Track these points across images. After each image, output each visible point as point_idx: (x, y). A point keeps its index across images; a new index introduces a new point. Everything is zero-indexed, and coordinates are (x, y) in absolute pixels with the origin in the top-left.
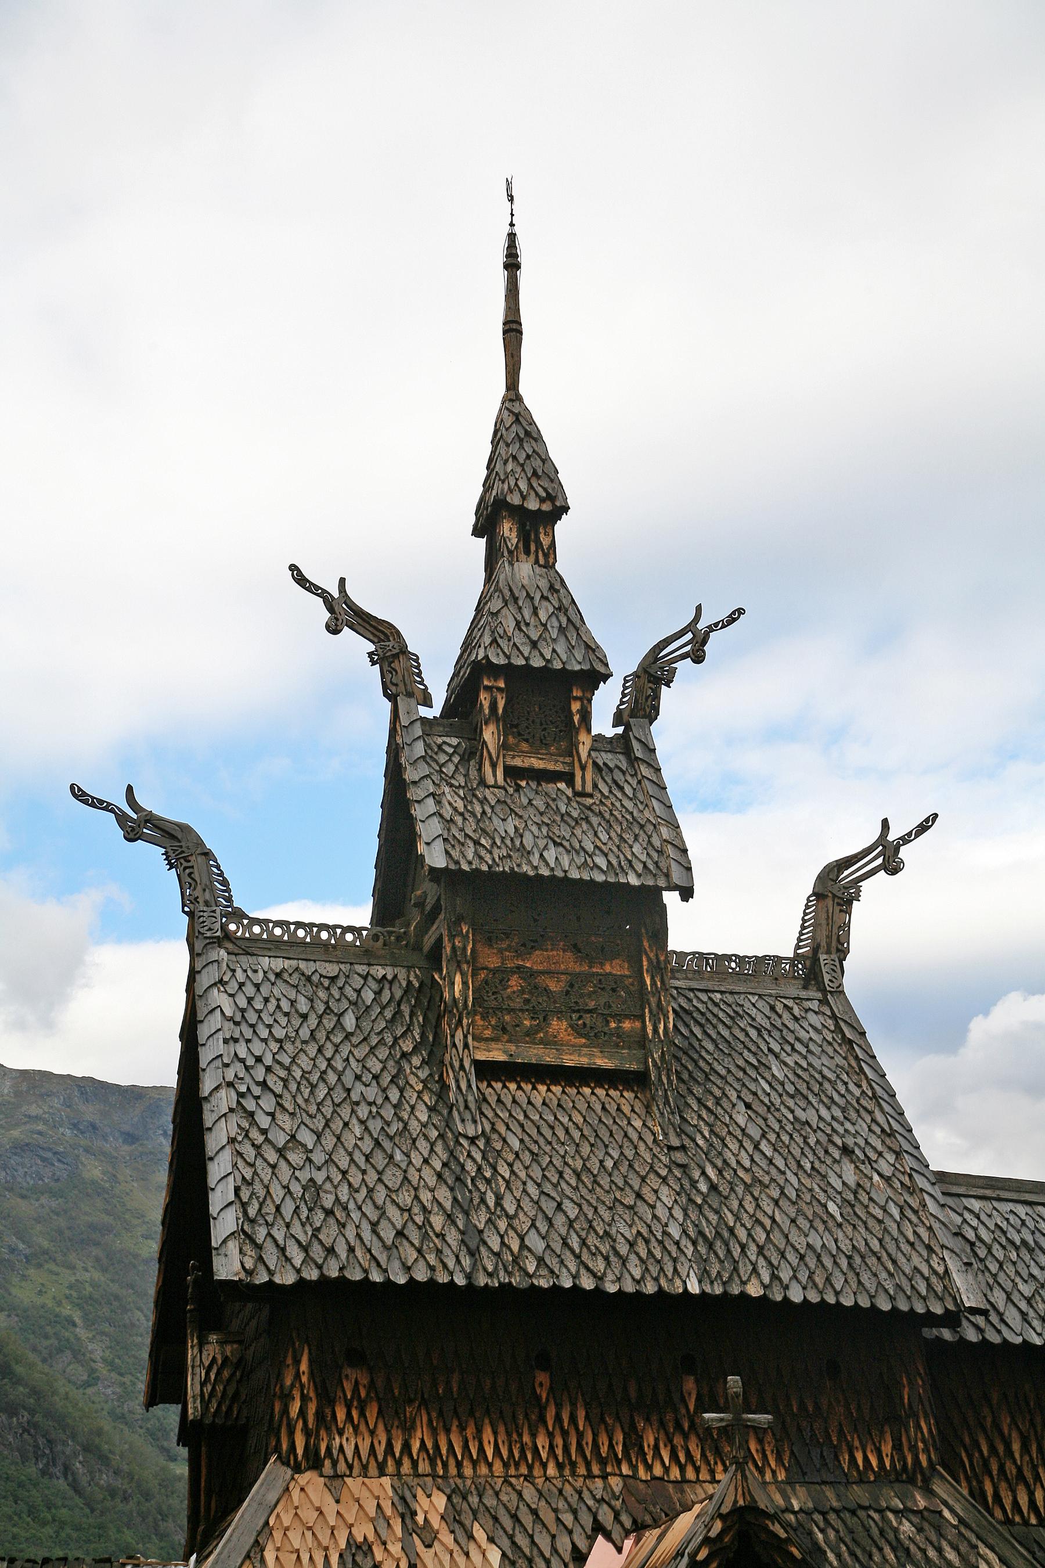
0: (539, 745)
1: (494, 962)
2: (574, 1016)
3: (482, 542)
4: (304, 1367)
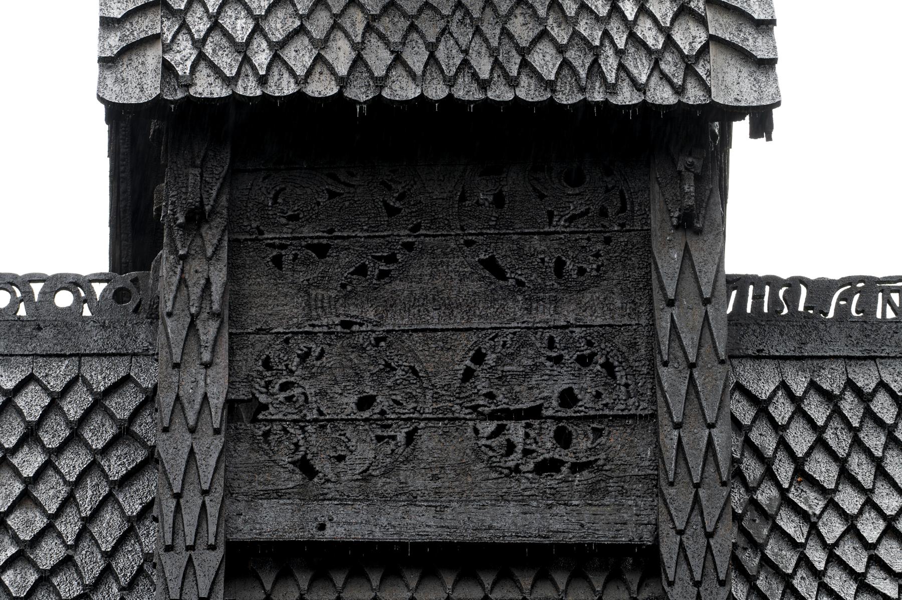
2: (489, 427)
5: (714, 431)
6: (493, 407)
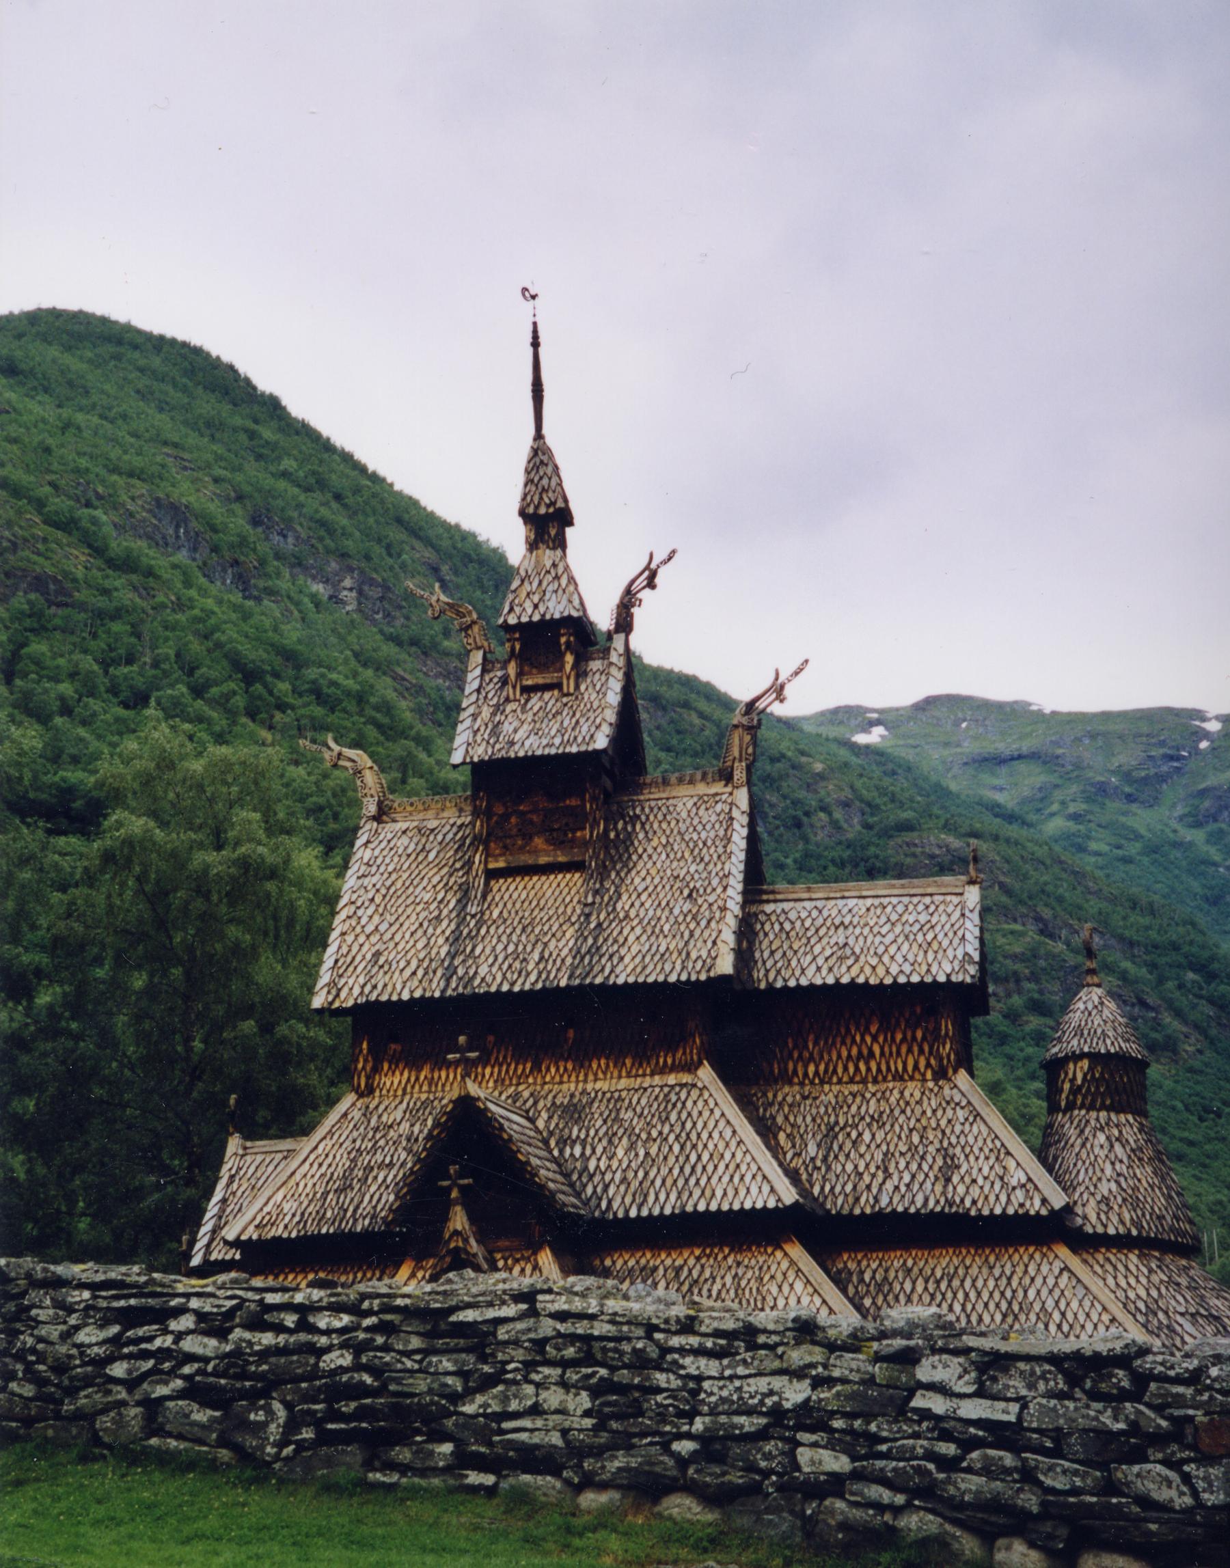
0: (542, 668)
4: (365, 1045)
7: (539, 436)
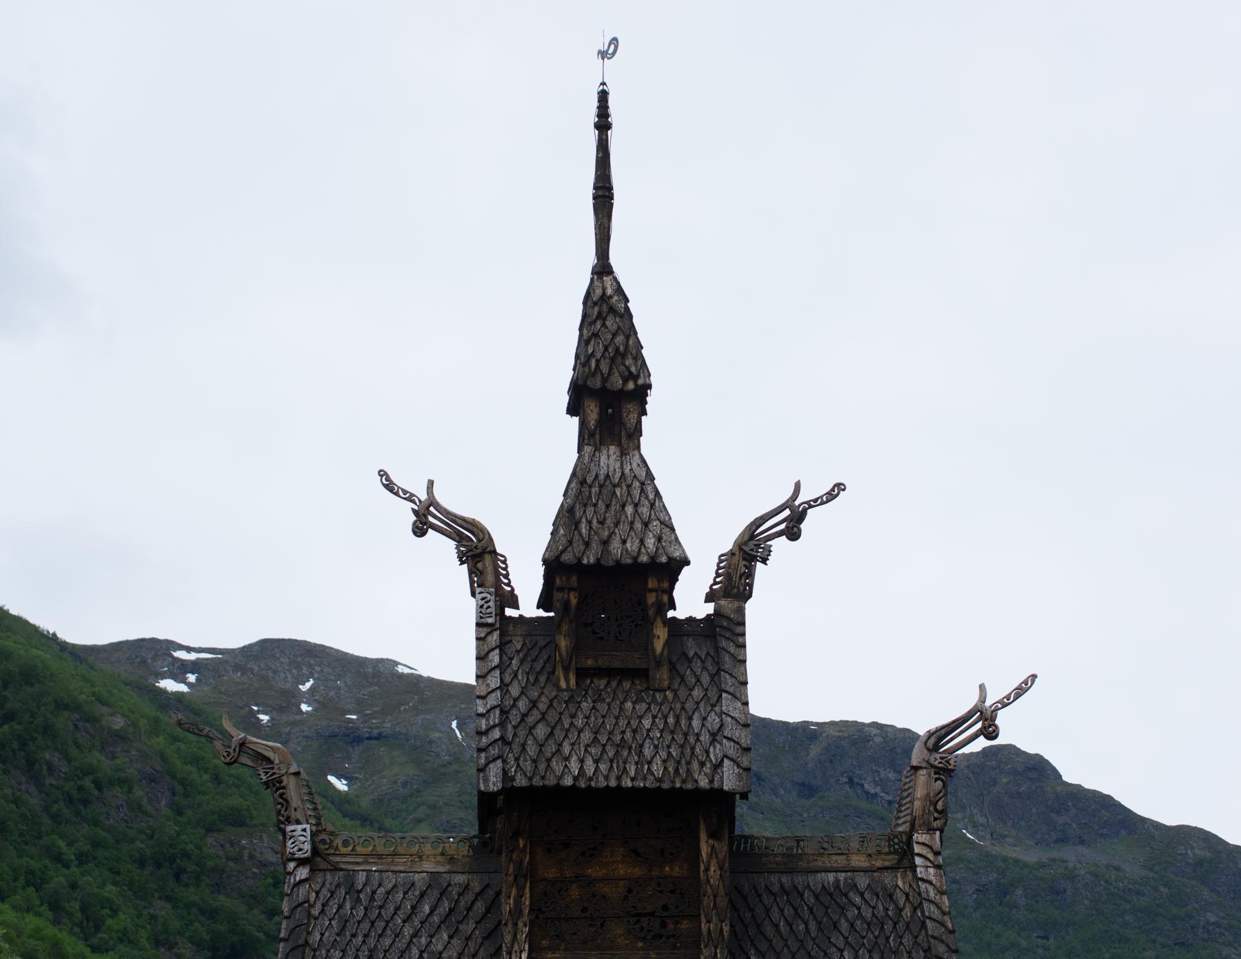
1: (552, 874)
2: (632, 920)
3: (576, 420)
5: (724, 924)
6: (635, 912)
7: (603, 269)
